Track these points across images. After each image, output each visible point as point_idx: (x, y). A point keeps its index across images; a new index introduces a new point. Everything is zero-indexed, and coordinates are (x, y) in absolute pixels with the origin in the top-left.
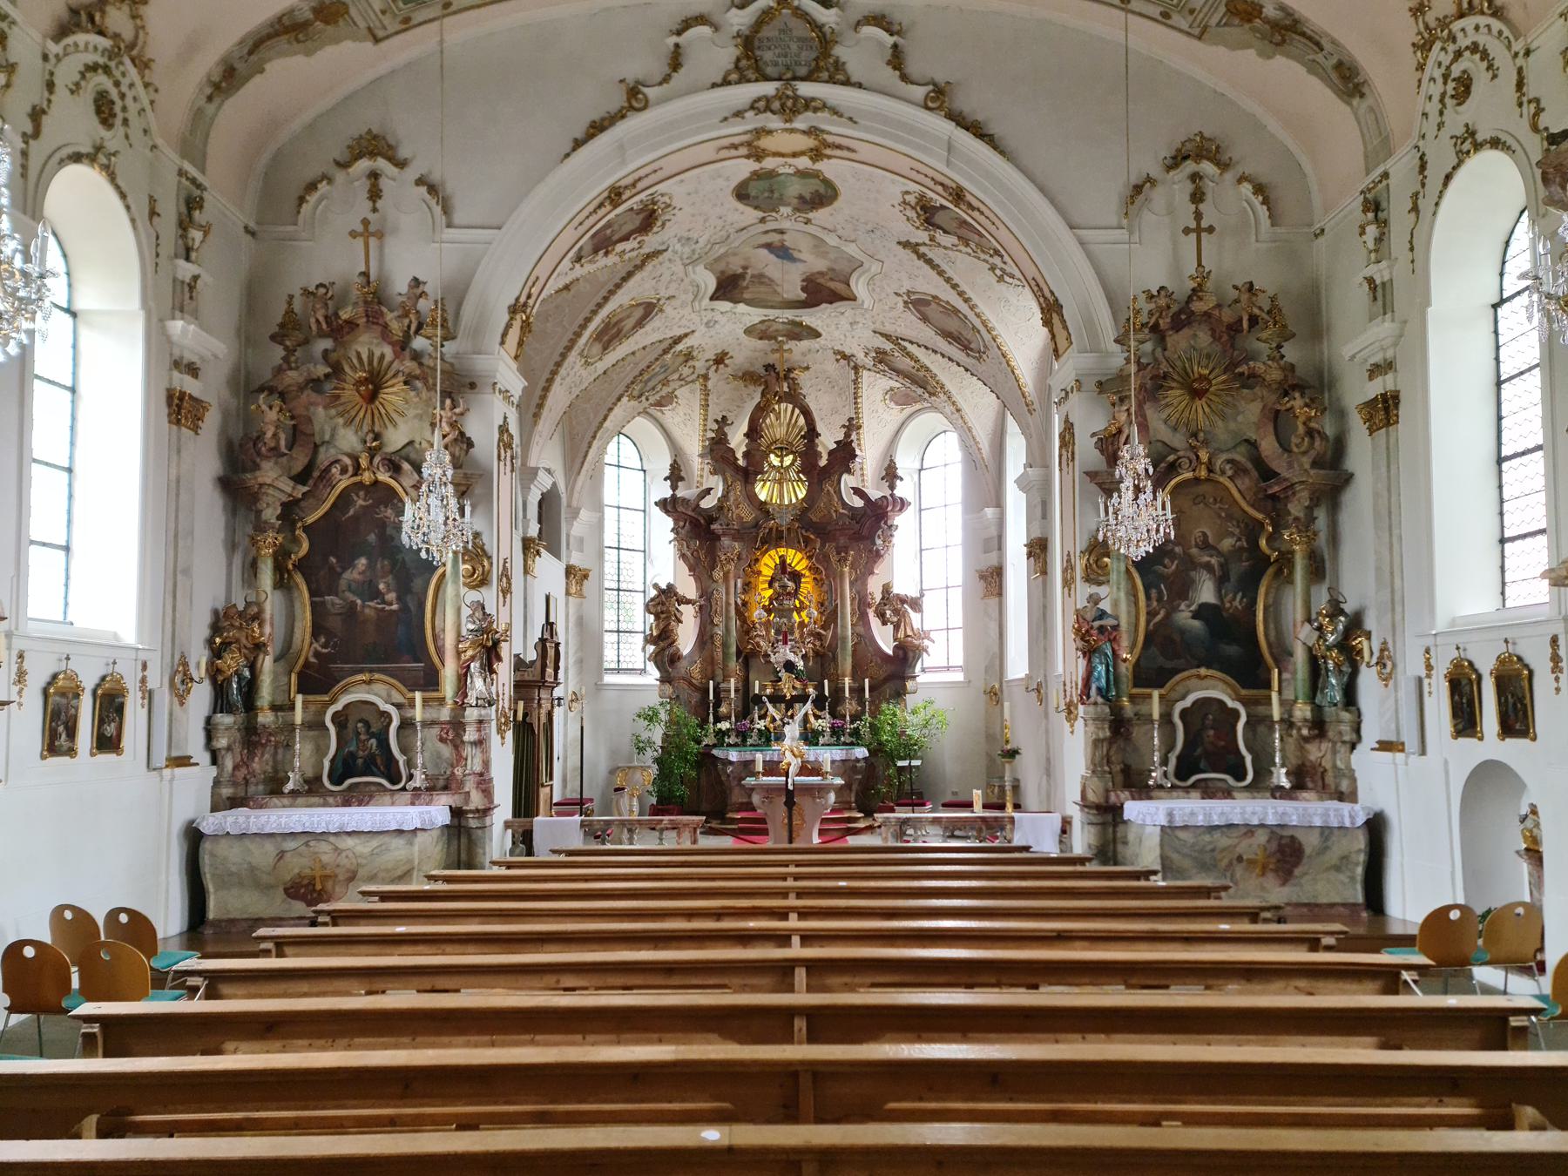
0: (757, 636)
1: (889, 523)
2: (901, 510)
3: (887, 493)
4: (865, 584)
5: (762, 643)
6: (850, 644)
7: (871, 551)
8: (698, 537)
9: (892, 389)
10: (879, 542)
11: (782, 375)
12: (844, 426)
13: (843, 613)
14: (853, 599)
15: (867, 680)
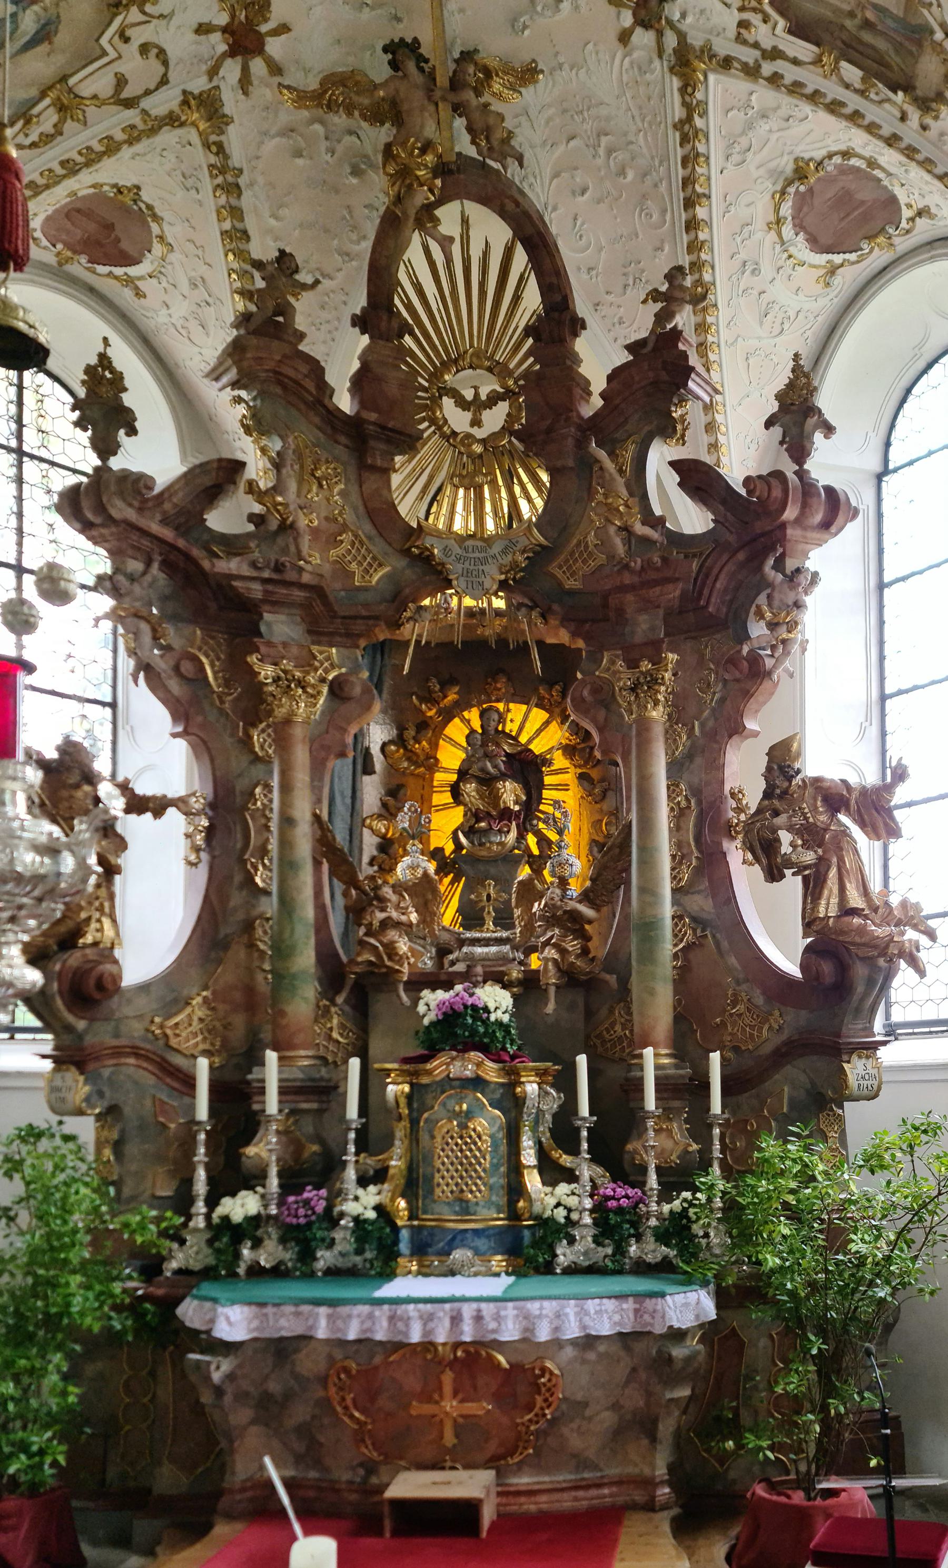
0: (386, 924)
1: (790, 564)
2: (826, 525)
3: (789, 469)
4: (716, 766)
5: (403, 946)
6: (667, 947)
7: (733, 661)
8: (198, 616)
9: (800, 174)
10: (757, 629)
11: (442, 80)
12: (655, 295)
13: (648, 853)
14: (678, 814)
15: (715, 1058)
